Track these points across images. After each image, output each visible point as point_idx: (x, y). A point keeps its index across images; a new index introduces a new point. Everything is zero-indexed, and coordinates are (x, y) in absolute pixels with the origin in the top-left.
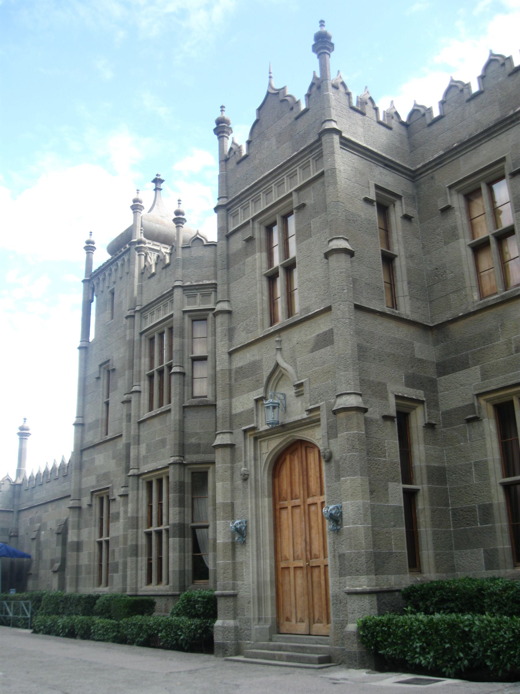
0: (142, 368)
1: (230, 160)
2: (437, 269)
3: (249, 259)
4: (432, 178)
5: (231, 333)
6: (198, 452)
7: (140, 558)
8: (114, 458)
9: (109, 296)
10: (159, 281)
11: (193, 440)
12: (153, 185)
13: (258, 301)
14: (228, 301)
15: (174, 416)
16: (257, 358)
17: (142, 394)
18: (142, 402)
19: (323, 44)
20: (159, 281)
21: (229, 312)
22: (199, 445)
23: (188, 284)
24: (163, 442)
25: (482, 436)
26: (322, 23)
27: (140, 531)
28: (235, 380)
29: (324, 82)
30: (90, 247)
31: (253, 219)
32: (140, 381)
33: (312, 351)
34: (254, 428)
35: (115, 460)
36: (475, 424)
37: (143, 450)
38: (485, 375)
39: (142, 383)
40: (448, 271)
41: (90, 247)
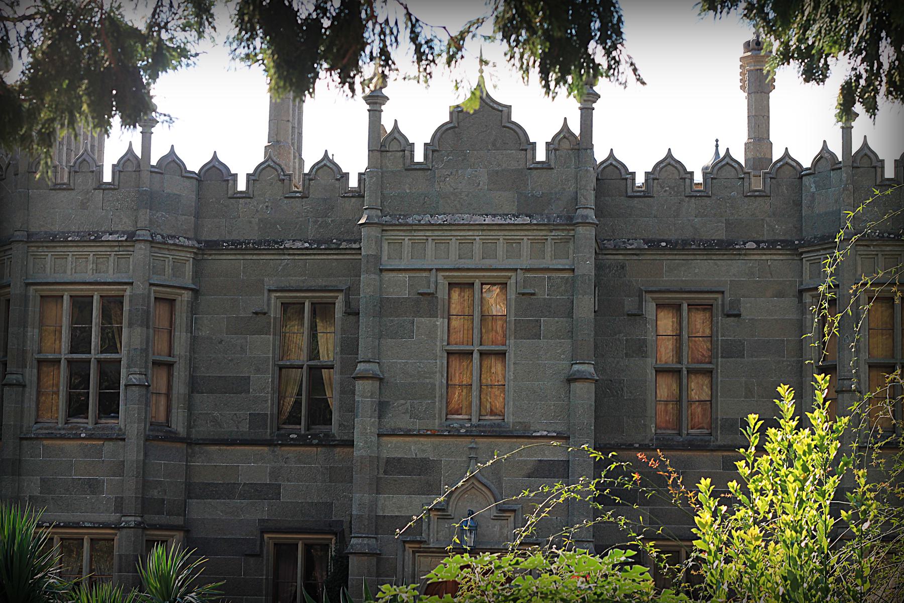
3: (424, 321)
4: (623, 267)
6: (160, 513)
10: (83, 206)
11: (155, 494)
13: (437, 383)
15: (132, 453)
17: (27, 390)
20: (83, 206)
21: (381, 380)
22: (163, 500)
24: (93, 486)
28: (385, 472)
29: (589, 151)
31: (437, 270)
32: (24, 366)
34: (420, 542)
39: (27, 370)
40: (625, 389)
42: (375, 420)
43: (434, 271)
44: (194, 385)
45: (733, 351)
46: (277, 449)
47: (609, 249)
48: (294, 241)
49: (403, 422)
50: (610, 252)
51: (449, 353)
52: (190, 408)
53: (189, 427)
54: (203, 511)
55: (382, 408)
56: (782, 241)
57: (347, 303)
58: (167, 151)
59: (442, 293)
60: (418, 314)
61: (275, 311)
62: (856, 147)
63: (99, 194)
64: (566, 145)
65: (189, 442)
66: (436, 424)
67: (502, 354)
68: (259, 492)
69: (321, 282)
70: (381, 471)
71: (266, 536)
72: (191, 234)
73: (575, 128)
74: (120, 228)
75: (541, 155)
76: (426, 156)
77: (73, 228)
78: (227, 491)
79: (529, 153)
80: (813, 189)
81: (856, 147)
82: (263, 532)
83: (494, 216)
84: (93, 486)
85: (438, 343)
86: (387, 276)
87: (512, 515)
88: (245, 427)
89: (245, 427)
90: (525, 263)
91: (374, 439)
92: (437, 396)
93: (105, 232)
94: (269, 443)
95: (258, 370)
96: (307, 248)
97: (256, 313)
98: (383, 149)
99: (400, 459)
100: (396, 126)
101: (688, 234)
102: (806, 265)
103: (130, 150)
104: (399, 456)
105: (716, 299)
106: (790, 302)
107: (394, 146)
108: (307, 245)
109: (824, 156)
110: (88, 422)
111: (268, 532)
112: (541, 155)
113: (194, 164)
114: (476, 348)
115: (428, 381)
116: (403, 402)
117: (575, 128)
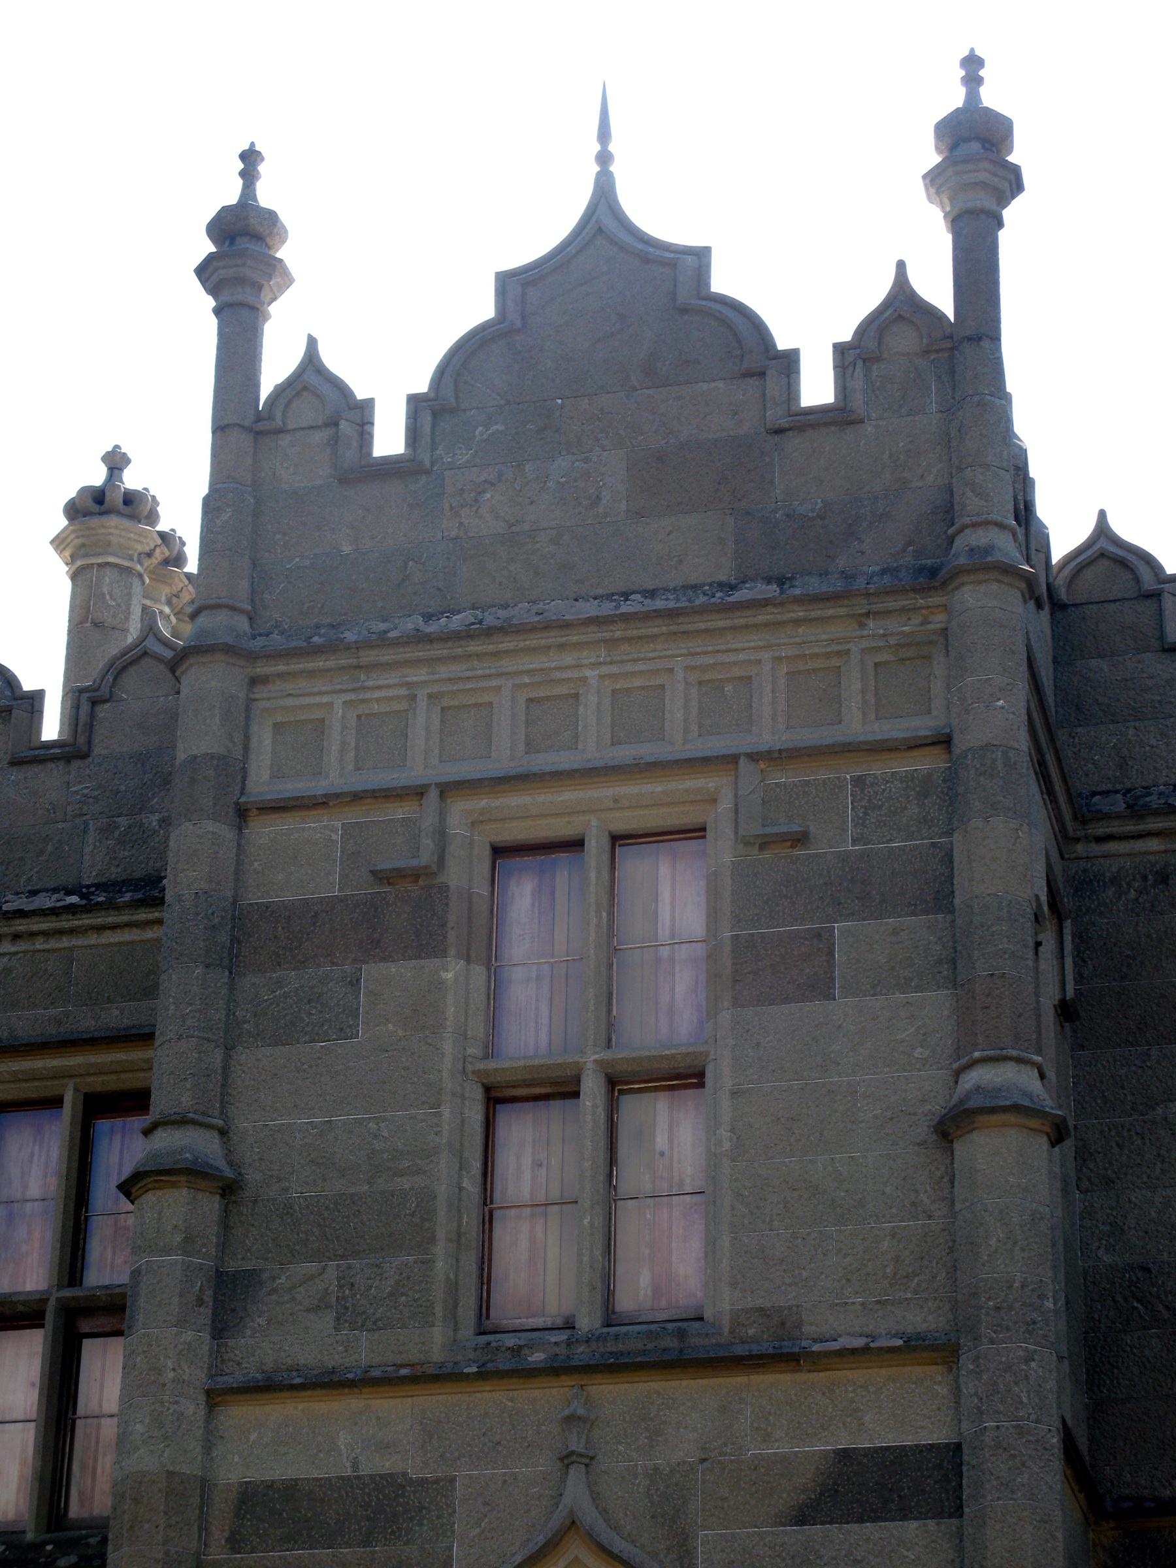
1: (285, 441)
2: (1146, 1269)
5: (228, 1297)
13: (443, 1190)
14: (223, 1133)
16: (411, 1464)
19: (977, 165)
26: (972, 65)
28: (235, 1542)
29: (985, 344)
31: (447, 789)
33: (802, 1516)
42: (197, 1337)
43: (433, 794)
47: (1108, 816)
48: (33, 893)
49: (312, 1342)
50: (1114, 828)
51: (497, 1098)
59: (465, 872)
64: (904, 341)
66: (434, 1343)
70: (219, 1536)
73: (937, 289)
75: (817, 387)
76: (413, 434)
79: (773, 384)
83: (652, 594)
85: (448, 1047)
86: (263, 830)
90: (767, 737)
91: (193, 1408)
92: (441, 1234)
96: (71, 909)
98: (260, 426)
99: (290, 1490)
100: (311, 360)
104: (290, 1474)
107: (306, 413)
108: (74, 899)
112: (817, 387)
114: (591, 1059)
115: (405, 1183)
116: (313, 1267)
117: (937, 289)
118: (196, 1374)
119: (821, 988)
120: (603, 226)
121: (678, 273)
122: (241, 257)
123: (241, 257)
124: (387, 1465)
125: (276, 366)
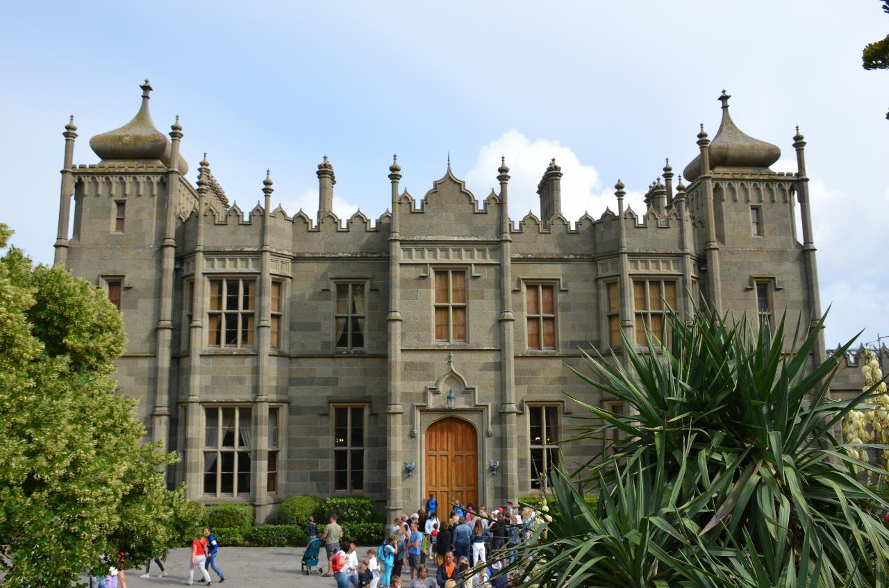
0: (205, 306)
7: (199, 474)
8: (129, 374)
9: (114, 205)
10: (234, 233)
12: (141, 92)
17: (204, 329)
18: (204, 337)
19: (503, 175)
23: (274, 250)
25: (525, 423)
27: (200, 449)
28: (405, 369)
30: (70, 133)
31: (430, 264)
33: (481, 370)
35: (133, 378)
36: (522, 416)
37: (207, 381)
38: (530, 391)
41: (70, 133)
44: (292, 327)
45: (566, 308)
46: (337, 360)
52: (290, 338)
53: (290, 349)
54: (296, 392)
55: (403, 335)
56: (587, 255)
57: (372, 285)
58: (277, 206)
60: (422, 287)
61: (333, 288)
62: (625, 208)
63: (243, 227)
65: (290, 357)
67: (463, 309)
68: (326, 382)
69: (357, 274)
71: (331, 405)
72: (290, 249)
73: (498, 192)
74: (254, 244)
77: (228, 244)
78: (310, 381)
80: (602, 229)
81: (625, 208)
82: (330, 402)
84: (240, 380)
87: (472, 391)
88: (319, 348)
89: (319, 348)
93: (245, 247)
94: (332, 357)
95: (325, 319)
97: (324, 290)
99: (412, 363)
101: (541, 250)
102: (600, 267)
103: (259, 205)
105: (555, 283)
106: (591, 284)
109: (608, 215)
110: (239, 347)
111: (332, 403)
113: (291, 215)
118: (399, 347)
119: (483, 298)
120: (449, 178)
121: (459, 184)
122: (394, 175)
123: (394, 175)
124: (426, 360)
125: (400, 192)
